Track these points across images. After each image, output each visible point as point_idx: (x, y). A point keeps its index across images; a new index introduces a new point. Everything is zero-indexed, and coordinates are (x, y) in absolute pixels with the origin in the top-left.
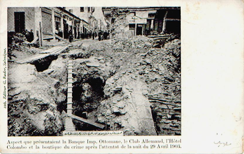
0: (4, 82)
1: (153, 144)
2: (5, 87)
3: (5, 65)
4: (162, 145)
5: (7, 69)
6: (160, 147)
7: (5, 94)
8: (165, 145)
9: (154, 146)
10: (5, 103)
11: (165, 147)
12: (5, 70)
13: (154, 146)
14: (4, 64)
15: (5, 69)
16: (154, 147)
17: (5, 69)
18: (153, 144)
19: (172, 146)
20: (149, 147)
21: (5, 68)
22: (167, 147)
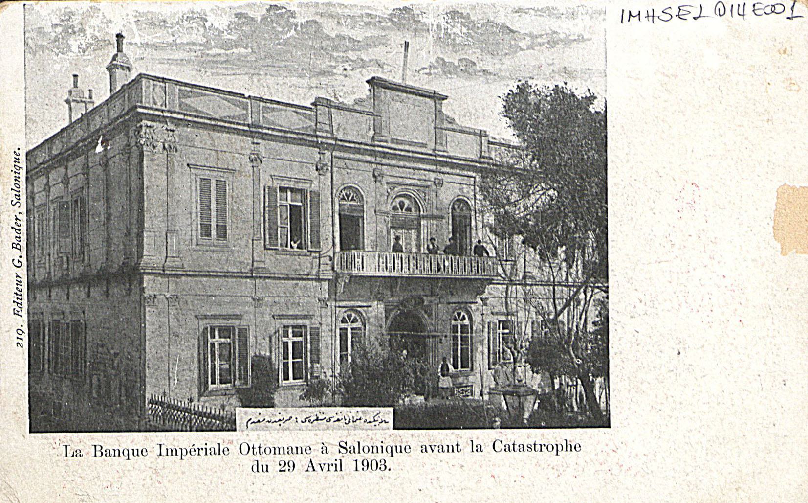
0: (16, 262)
1: (287, 458)
2: (17, 276)
3: (18, 204)
4: (322, 463)
5: (23, 218)
6: (317, 468)
7: (19, 301)
8: (334, 462)
9: (291, 464)
10: (20, 331)
11: (332, 468)
12: (18, 222)
13: (291, 464)
14: (15, 201)
15: (17, 219)
16: (291, 469)
17: (17, 219)
18: (287, 458)
19: (360, 466)
20: (274, 468)
21: (19, 216)
22: (339, 468)
